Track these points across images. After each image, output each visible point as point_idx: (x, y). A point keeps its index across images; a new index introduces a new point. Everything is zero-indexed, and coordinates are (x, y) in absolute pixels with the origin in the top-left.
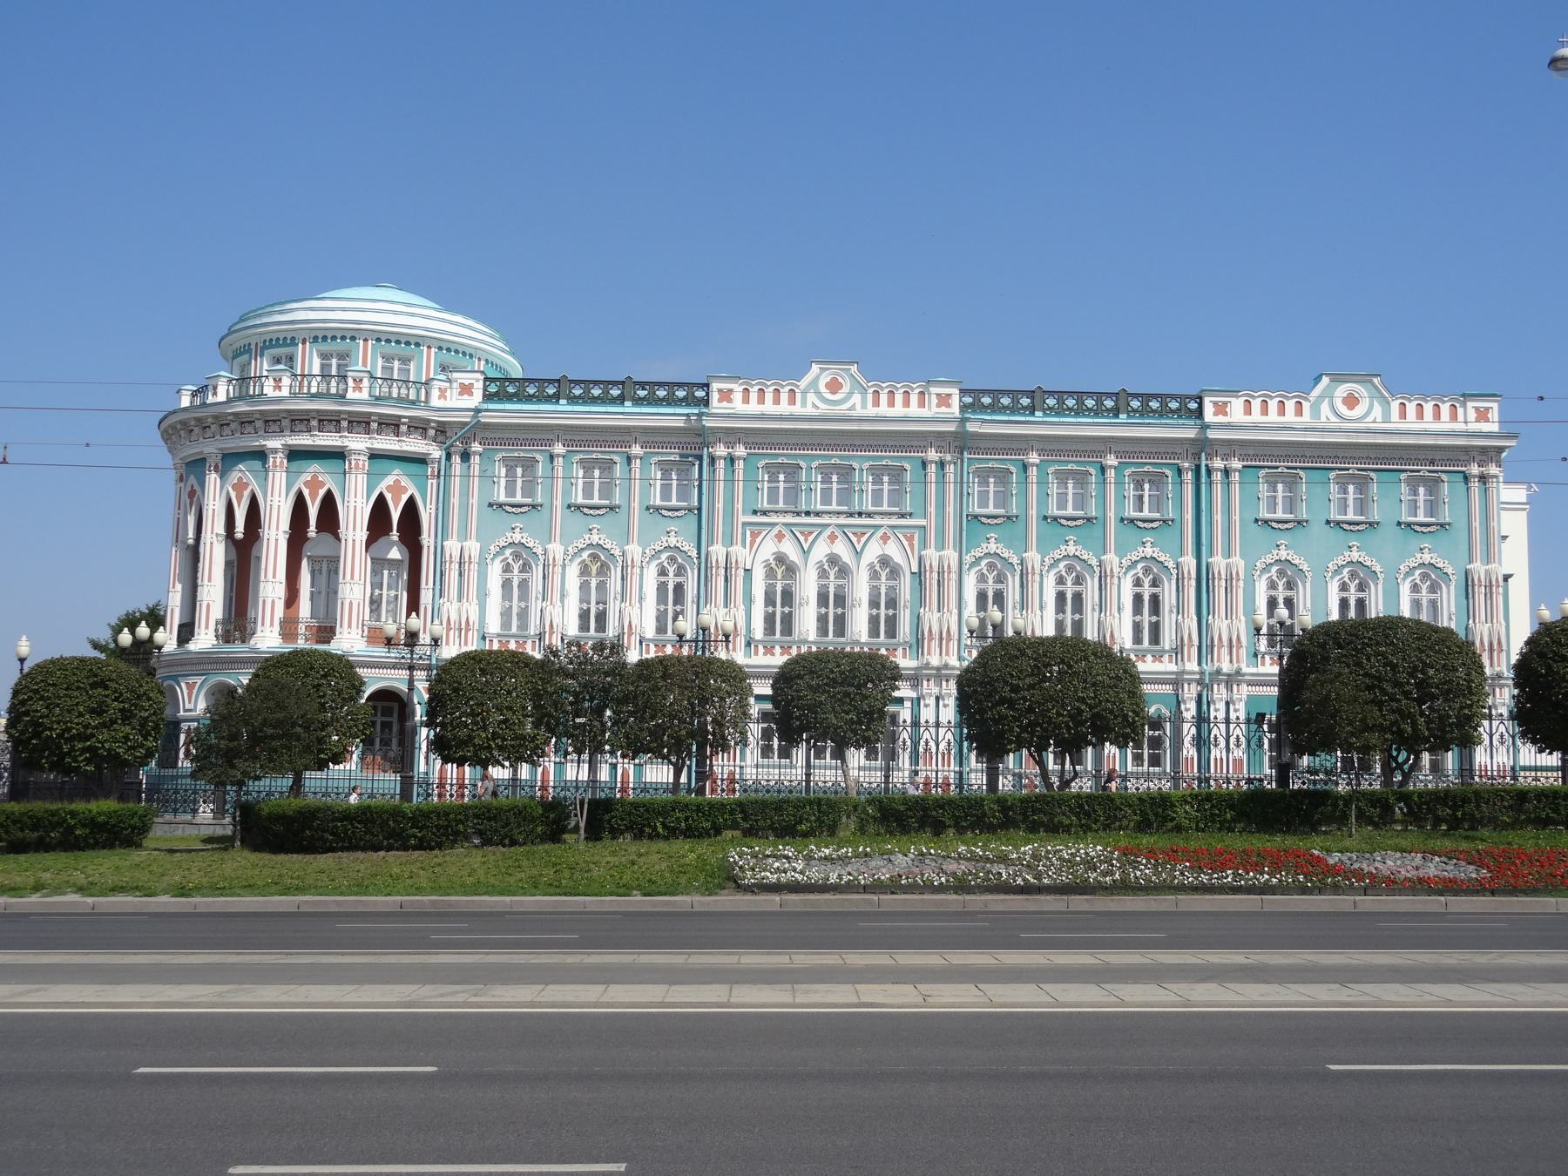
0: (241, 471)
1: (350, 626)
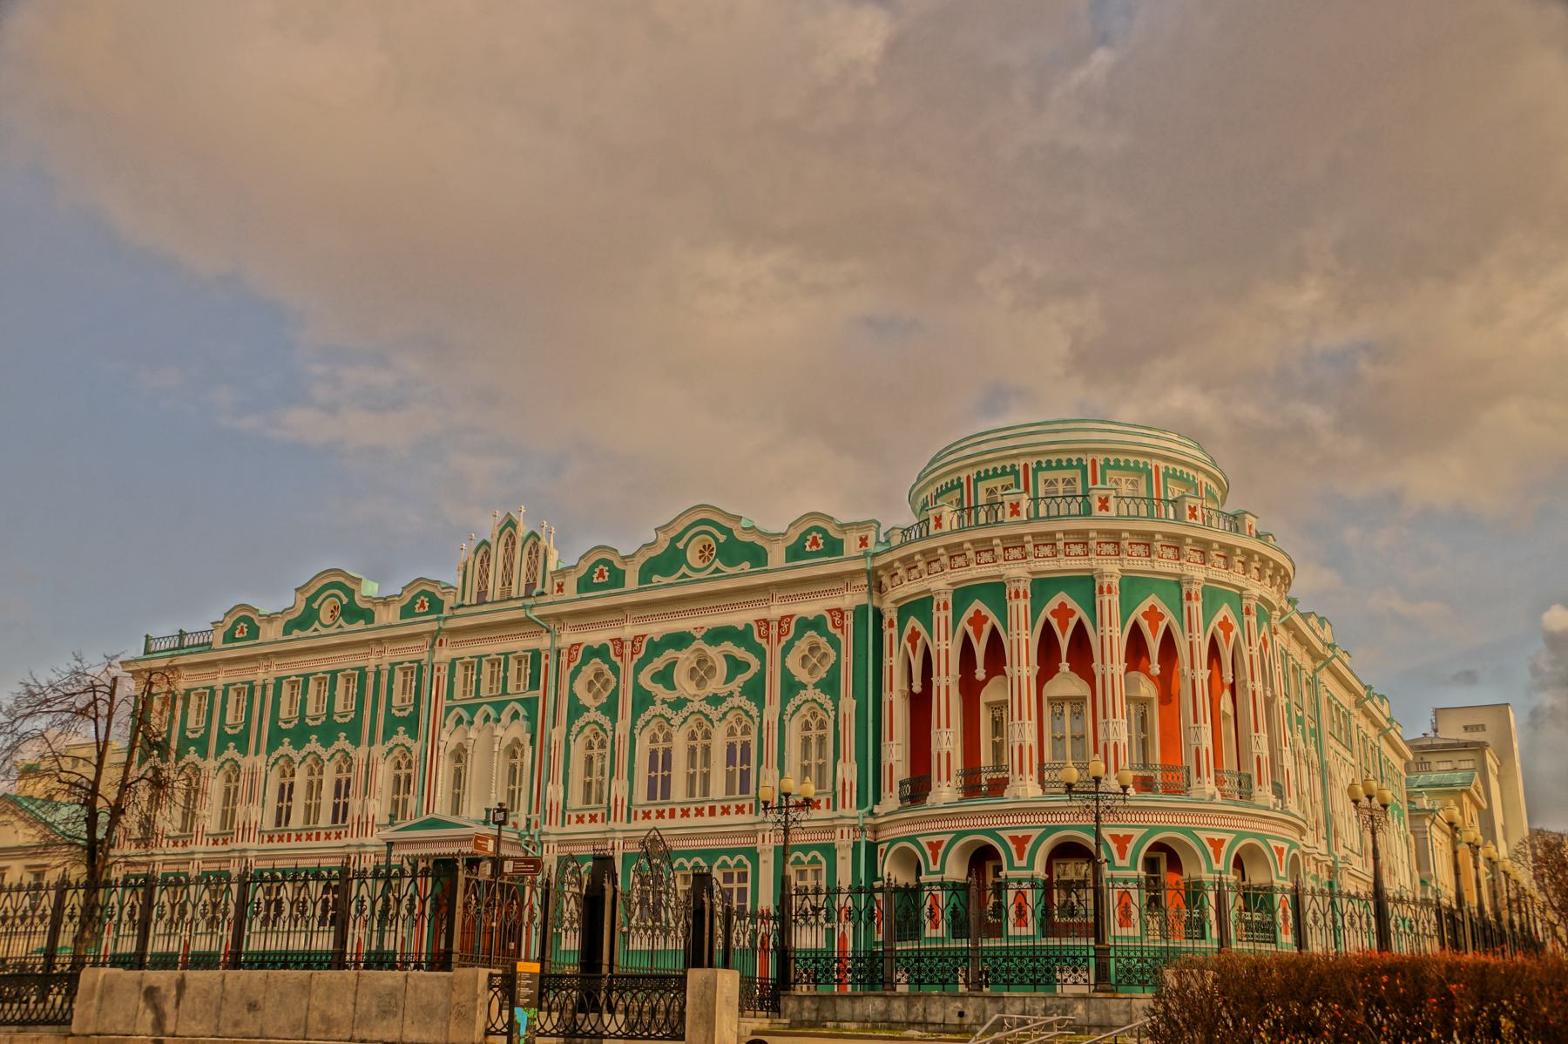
0: (913, 622)
1: (1021, 771)
